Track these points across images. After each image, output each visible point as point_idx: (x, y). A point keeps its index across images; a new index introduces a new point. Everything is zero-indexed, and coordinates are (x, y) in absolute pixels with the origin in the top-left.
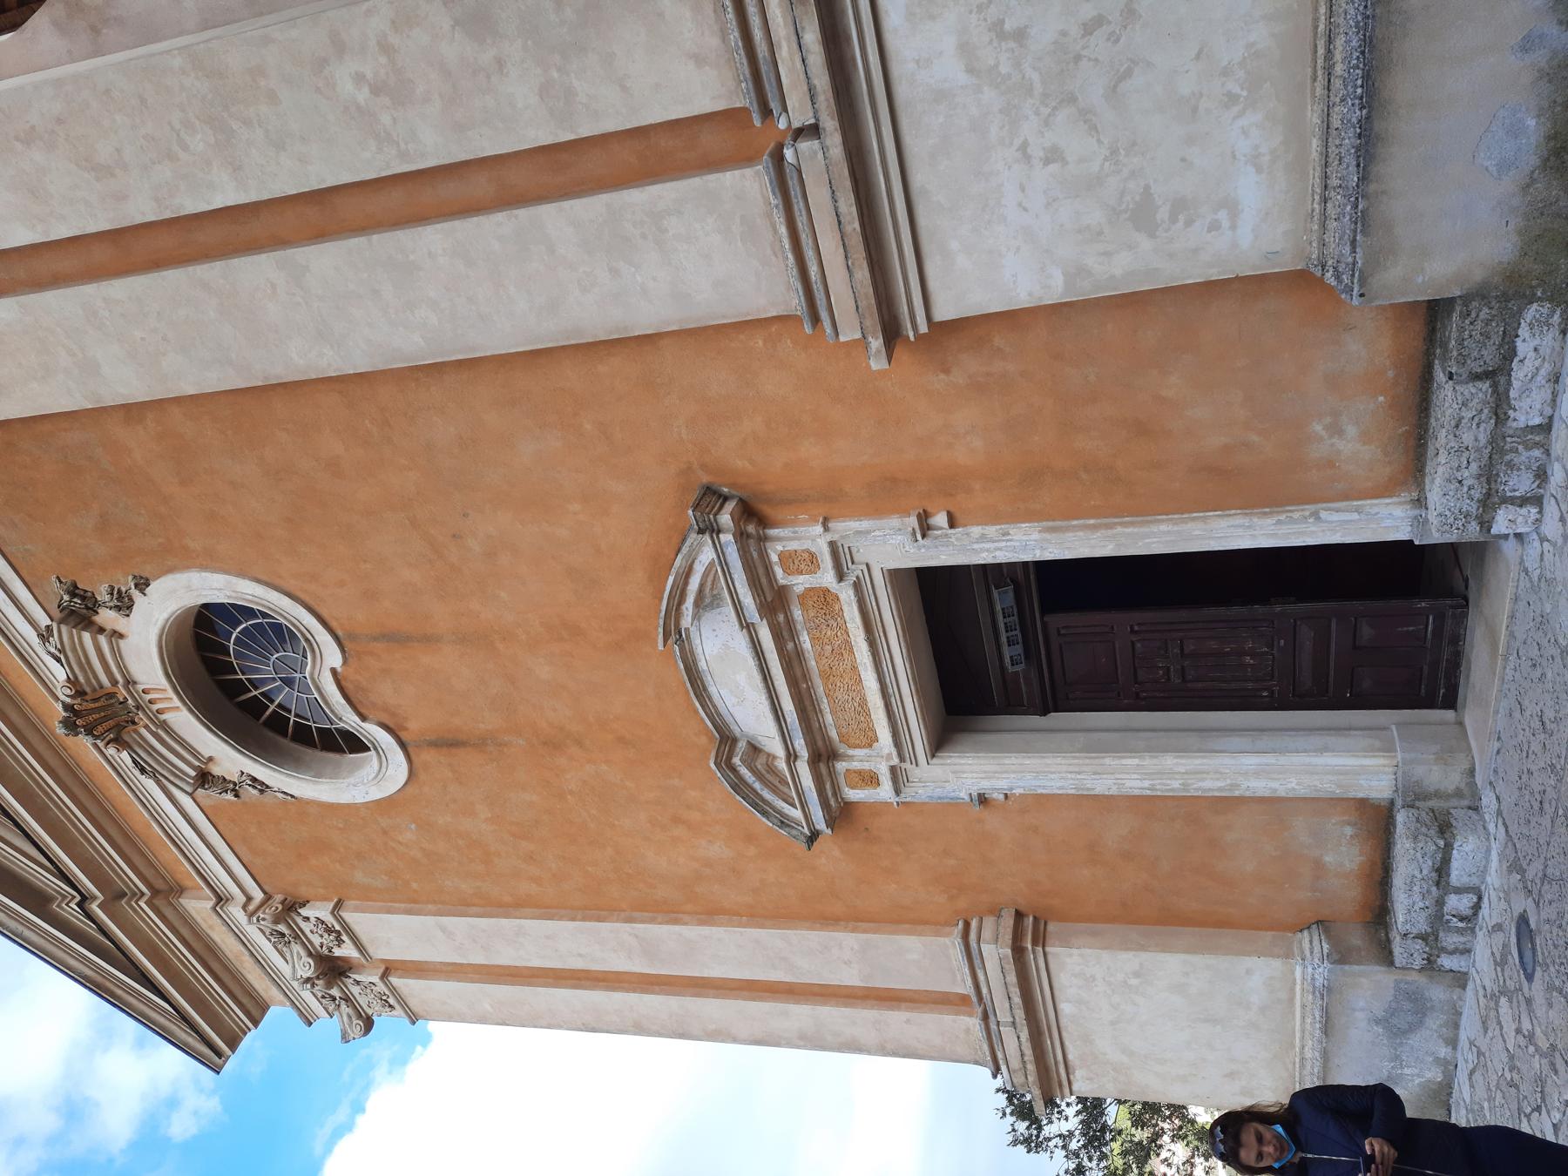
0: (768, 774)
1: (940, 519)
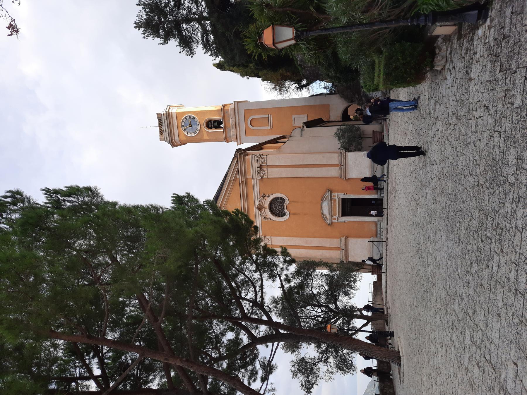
0: (326, 217)
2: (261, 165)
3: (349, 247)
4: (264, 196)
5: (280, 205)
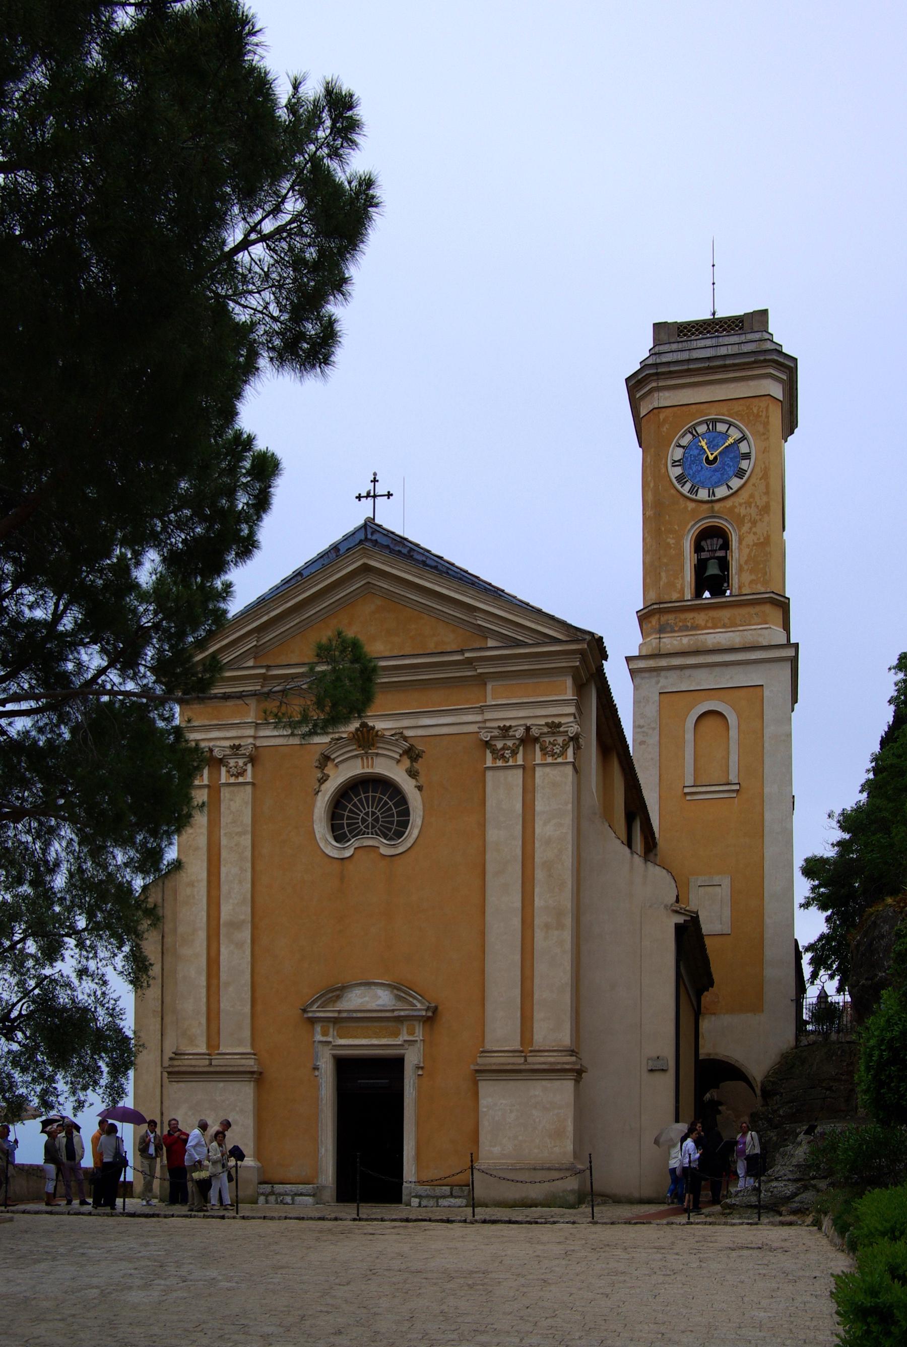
1: (420, 1072)
2: (536, 740)
3: (221, 1085)
4: (412, 754)
5: (377, 820)
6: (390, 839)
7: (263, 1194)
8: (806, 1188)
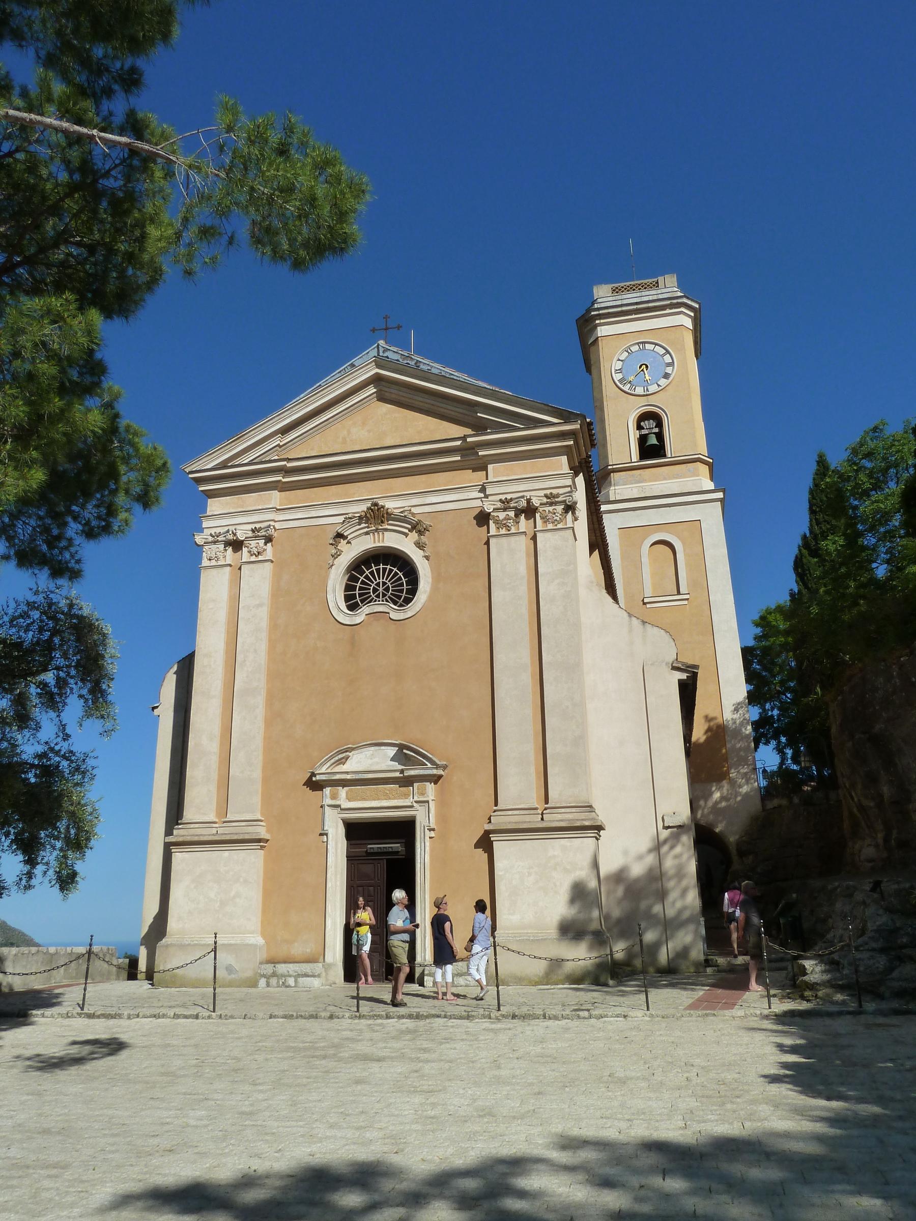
5: (387, 589)
6: (401, 606)
7: (264, 976)
8: (901, 960)
